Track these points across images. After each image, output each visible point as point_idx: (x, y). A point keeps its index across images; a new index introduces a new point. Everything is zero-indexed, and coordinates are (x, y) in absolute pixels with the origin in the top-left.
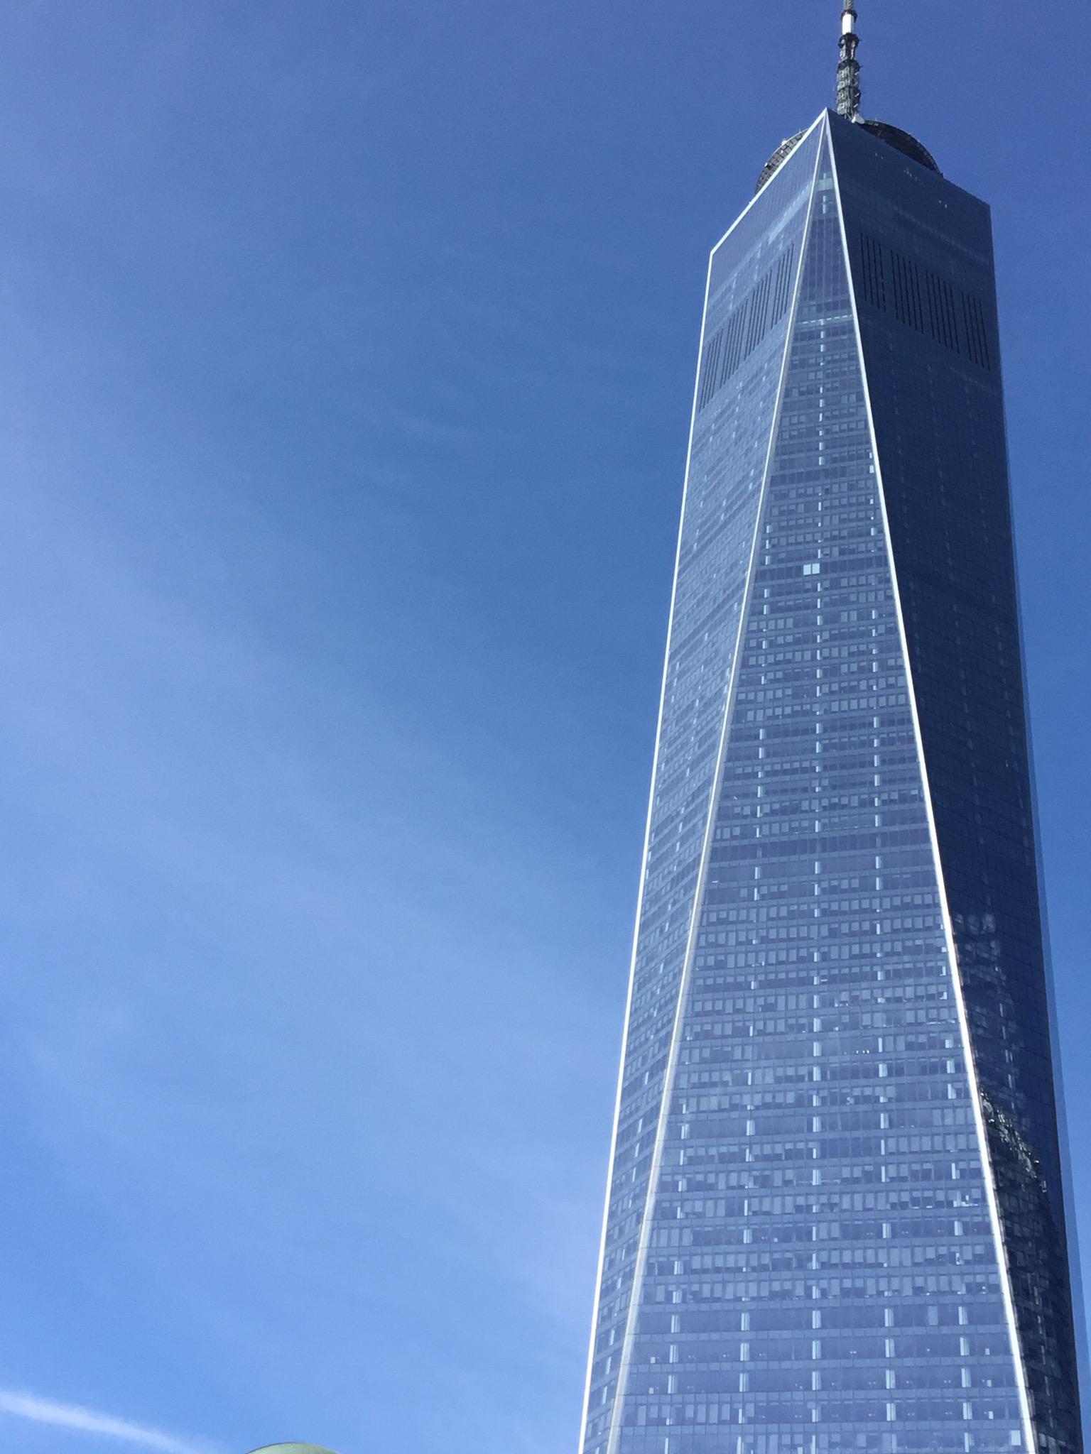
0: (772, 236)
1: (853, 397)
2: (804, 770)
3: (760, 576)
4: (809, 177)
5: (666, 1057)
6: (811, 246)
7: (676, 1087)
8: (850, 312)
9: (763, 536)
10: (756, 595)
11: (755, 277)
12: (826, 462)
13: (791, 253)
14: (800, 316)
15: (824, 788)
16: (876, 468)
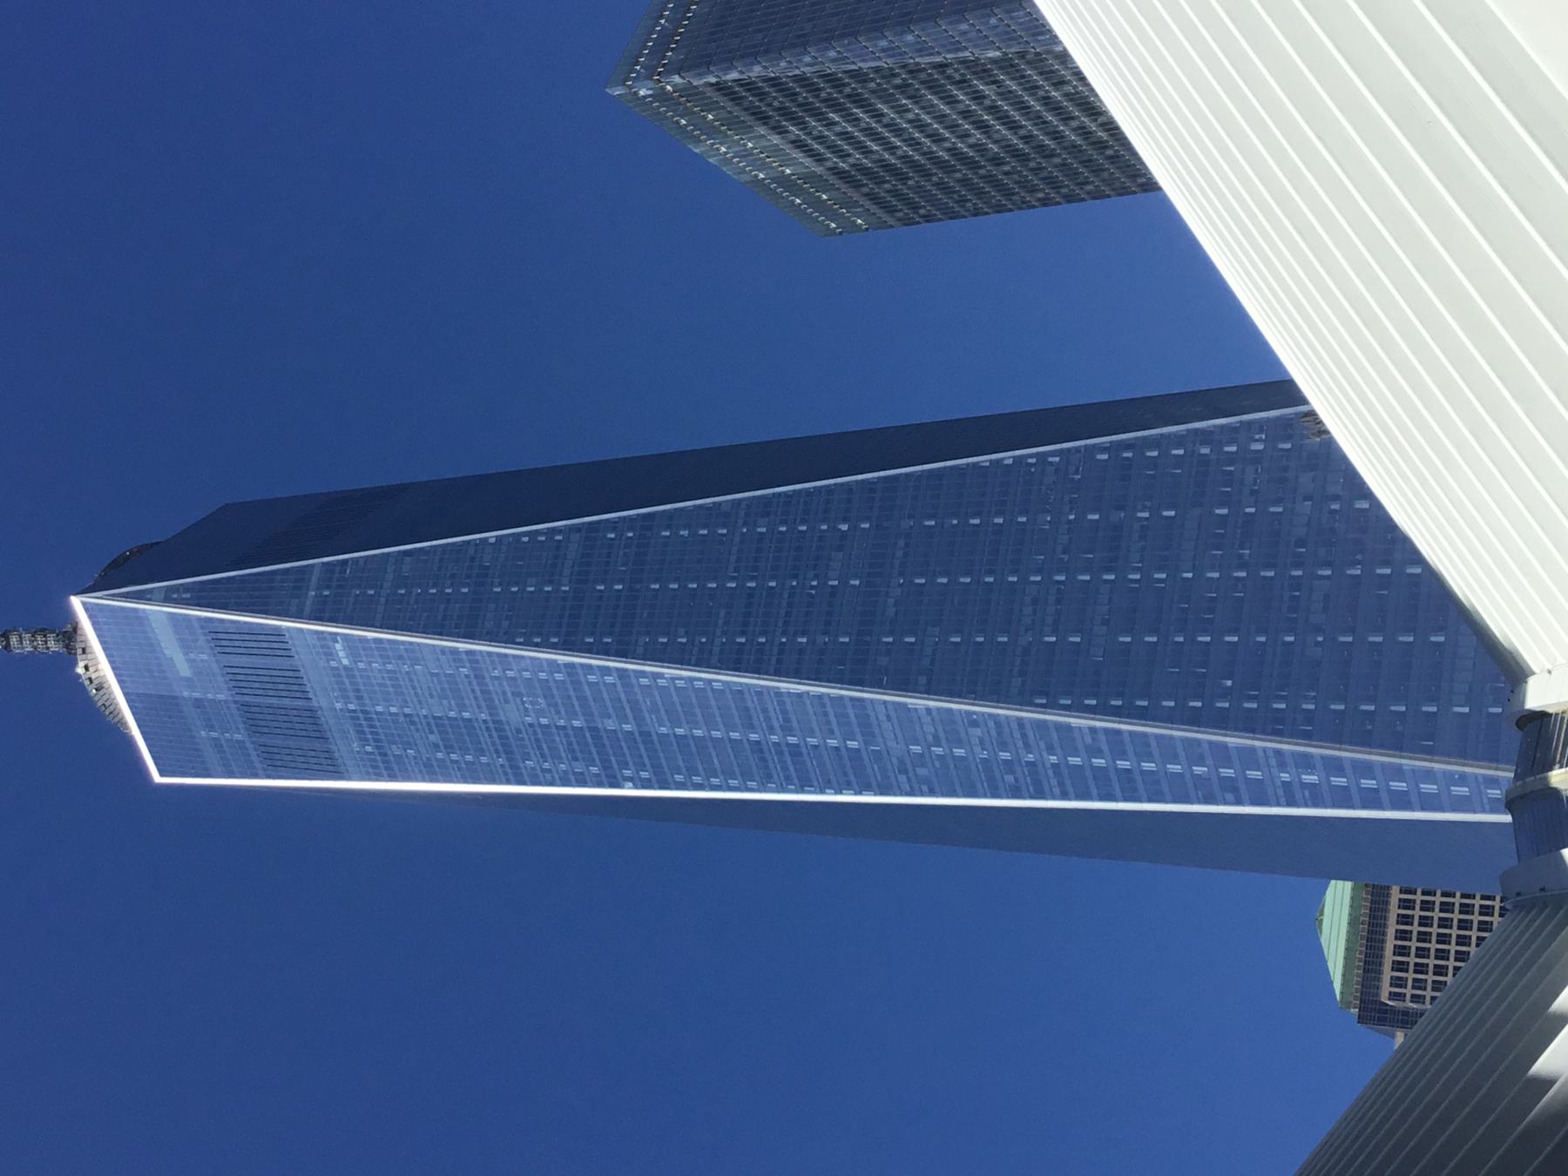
0: (185, 670)
1: (408, 559)
2: (791, 595)
3: (568, 646)
4: (139, 619)
5: (1060, 727)
6: (224, 607)
7: (1092, 711)
8: (312, 566)
9: (528, 644)
10: (589, 650)
11: (220, 697)
12: (467, 585)
13: (218, 636)
14: (298, 616)
15: (816, 577)
16: (491, 535)
